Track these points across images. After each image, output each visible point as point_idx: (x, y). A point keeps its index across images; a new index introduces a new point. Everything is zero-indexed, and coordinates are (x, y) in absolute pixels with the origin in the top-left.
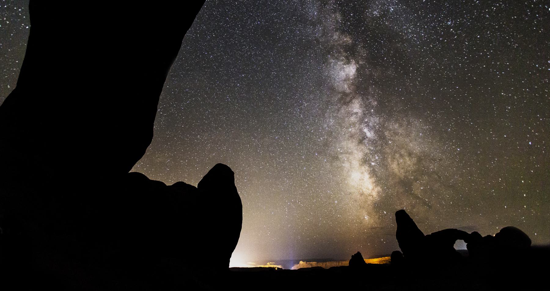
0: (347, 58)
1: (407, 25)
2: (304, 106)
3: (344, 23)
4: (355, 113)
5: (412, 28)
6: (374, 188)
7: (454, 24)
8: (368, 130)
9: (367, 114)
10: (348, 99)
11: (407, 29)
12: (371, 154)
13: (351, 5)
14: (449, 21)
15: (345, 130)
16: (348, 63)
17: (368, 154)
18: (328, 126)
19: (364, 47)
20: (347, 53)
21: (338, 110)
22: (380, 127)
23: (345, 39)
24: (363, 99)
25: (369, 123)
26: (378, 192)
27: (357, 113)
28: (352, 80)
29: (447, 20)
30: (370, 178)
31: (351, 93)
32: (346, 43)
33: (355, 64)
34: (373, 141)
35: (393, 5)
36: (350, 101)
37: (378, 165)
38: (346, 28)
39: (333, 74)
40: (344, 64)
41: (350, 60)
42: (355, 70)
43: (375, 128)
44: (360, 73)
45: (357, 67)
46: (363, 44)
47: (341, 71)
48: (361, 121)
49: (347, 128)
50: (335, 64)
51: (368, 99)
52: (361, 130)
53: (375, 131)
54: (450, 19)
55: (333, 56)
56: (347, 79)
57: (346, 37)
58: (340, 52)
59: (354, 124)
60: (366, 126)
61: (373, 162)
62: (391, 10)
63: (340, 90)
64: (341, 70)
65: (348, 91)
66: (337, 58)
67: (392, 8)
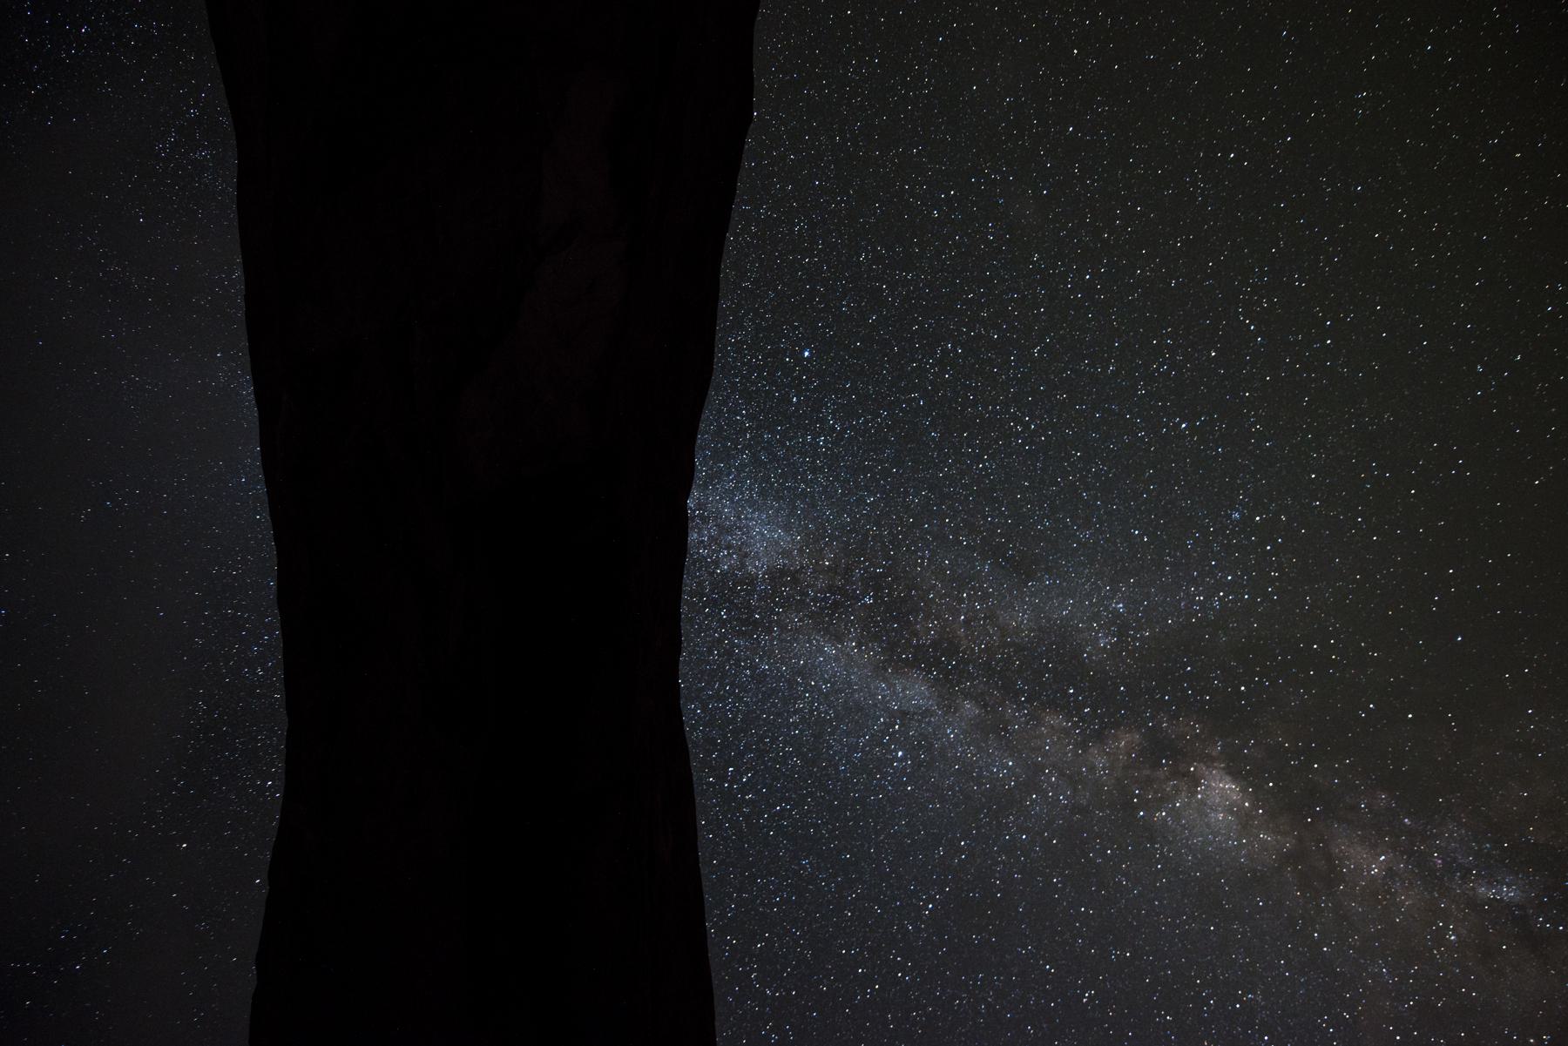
0: (1176, 773)
11: (1193, 602)
13: (1048, 678)
28: (1255, 807)
29: (1224, 517)
32: (1133, 748)
38: (1095, 724)
39: (1203, 842)
42: (1228, 778)
45: (1224, 769)
47: (1206, 816)
52: (1474, 904)
54: (1226, 511)
56: (1245, 822)
57: (1116, 738)
60: (1462, 878)
62: (1121, 608)
67: (1117, 603)
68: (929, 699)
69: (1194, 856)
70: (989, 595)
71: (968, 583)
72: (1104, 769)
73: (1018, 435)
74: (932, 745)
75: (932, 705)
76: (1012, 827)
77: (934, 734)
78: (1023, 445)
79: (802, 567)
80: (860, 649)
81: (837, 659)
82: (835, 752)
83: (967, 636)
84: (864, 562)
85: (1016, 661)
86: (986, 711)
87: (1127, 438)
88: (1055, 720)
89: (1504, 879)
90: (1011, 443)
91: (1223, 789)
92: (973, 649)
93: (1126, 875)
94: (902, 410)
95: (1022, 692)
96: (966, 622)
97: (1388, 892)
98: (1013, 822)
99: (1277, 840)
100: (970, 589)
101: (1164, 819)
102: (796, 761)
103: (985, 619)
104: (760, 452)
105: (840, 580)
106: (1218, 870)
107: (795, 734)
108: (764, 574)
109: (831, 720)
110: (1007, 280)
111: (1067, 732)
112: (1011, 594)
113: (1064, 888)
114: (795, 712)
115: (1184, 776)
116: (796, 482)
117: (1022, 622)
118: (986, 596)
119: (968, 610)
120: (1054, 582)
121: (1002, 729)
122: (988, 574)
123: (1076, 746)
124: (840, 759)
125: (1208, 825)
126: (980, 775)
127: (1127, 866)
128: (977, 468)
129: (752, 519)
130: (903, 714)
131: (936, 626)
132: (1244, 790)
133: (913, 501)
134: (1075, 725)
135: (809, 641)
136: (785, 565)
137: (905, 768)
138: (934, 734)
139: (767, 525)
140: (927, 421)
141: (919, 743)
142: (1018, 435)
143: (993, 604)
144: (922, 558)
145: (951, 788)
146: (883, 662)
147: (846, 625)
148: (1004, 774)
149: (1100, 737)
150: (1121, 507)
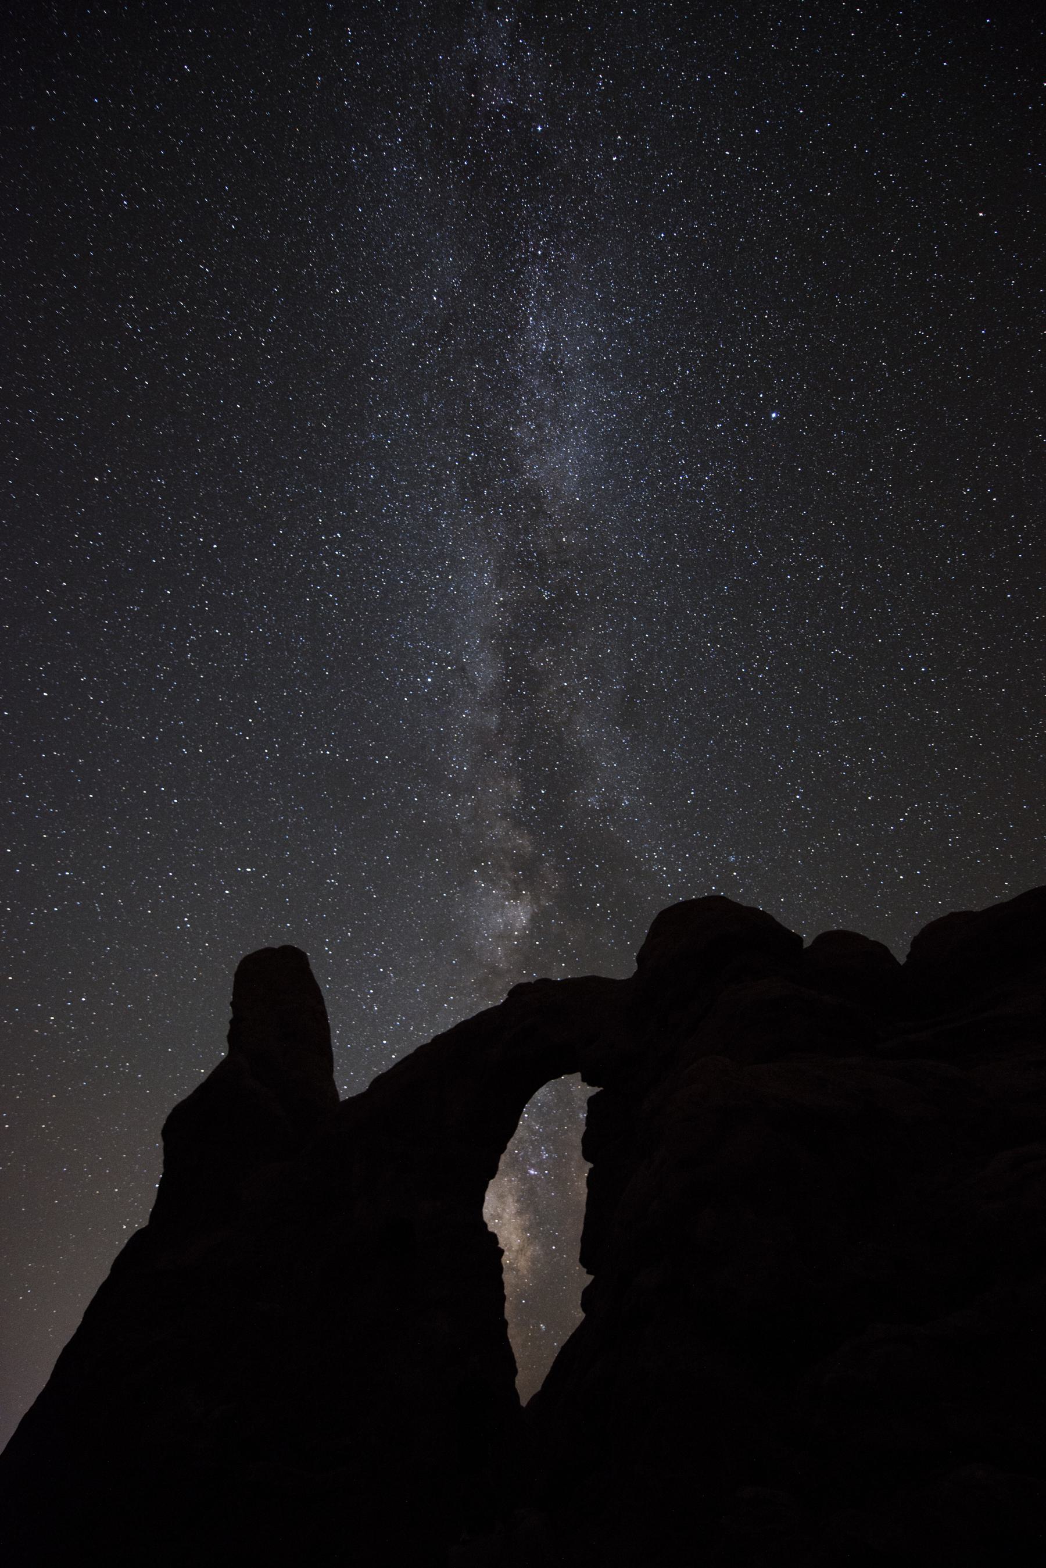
0: (515, 883)
1: (651, 841)
2: (389, 984)
3: (522, 806)
5: (661, 851)
6: (524, 1246)
7: (740, 862)
11: (650, 851)
12: (532, 1142)
13: (545, 771)
14: (732, 855)
16: (517, 896)
17: (526, 1141)
19: (557, 869)
20: (517, 872)
26: (534, 1260)
28: (517, 938)
30: (519, 1213)
31: (509, 971)
33: (530, 902)
34: (542, 1106)
35: (630, 794)
37: (545, 1175)
42: (529, 916)
44: (539, 928)
45: (534, 910)
54: (733, 850)
55: (484, 874)
56: (504, 936)
57: (521, 837)
61: (533, 1166)
62: (625, 803)
67: (628, 800)
69: (463, 914)
70: (594, 699)
73: (749, 666)
74: (449, 703)
75: (481, 689)
77: (459, 701)
78: (741, 674)
79: (550, 517)
80: (499, 607)
81: (482, 589)
82: (401, 625)
83: (550, 694)
86: (498, 734)
87: (773, 758)
88: (515, 788)
90: (740, 663)
91: (520, 916)
93: (427, 876)
94: (741, 546)
99: (501, 958)
100: (593, 681)
102: (377, 593)
103: (572, 703)
104: (651, 413)
106: (462, 930)
107: (399, 581)
108: (528, 480)
109: (426, 608)
111: (509, 799)
113: (395, 840)
114: (418, 573)
115: (516, 888)
116: (632, 469)
117: (582, 733)
120: (627, 746)
121: (488, 752)
122: (612, 690)
124: (399, 632)
125: (490, 915)
129: (577, 439)
130: (463, 669)
131: (548, 665)
132: (525, 928)
133: (654, 597)
134: (518, 804)
135: (485, 557)
136: (545, 497)
137: (419, 688)
138: (459, 701)
139: (577, 458)
140: (737, 577)
141: (446, 692)
142: (749, 666)
143: (587, 705)
145: (423, 731)
147: (515, 584)
149: (517, 824)
150: (710, 774)
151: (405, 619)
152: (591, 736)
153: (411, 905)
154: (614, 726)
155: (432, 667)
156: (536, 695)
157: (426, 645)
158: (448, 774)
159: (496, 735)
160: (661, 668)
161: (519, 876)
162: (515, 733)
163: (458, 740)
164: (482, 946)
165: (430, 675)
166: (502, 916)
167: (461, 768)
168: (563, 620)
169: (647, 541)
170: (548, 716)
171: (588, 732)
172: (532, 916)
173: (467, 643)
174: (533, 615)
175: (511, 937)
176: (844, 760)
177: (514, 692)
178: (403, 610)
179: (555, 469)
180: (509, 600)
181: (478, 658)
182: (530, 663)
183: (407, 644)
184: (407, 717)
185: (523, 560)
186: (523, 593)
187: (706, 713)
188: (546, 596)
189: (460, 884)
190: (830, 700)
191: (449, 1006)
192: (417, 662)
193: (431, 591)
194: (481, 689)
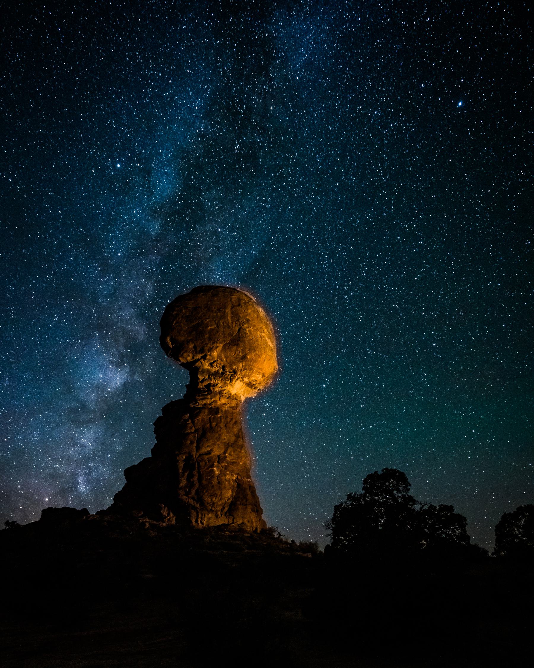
0: (122, 356)
4: (80, 444)
8: (85, 482)
9: (99, 457)
10: (83, 417)
15: (49, 461)
16: (119, 365)
18: (23, 440)
20: (126, 349)
21: (58, 425)
22: (104, 486)
23: (138, 327)
24: (106, 429)
25: (94, 471)
27: (85, 447)
28: (108, 393)
31: (94, 411)
32: (135, 335)
33: (128, 374)
34: (82, 501)
36: (88, 422)
40: (112, 363)
41: (125, 363)
42: (122, 382)
43: (97, 483)
46: (157, 354)
47: (100, 369)
48: (85, 460)
49: (55, 461)
50: (99, 353)
51: (113, 435)
52: (75, 475)
53: (94, 488)
58: (116, 341)
59: (69, 460)
60: (87, 473)
63: (82, 397)
64: (101, 367)
65: (91, 406)
66: (106, 347)
68: (160, 195)
69: (76, 360)
70: (234, 252)
71: (243, 237)
72: (121, 315)
73: (342, 286)
74: (127, 194)
75: (156, 197)
76: (76, 251)
77: (135, 198)
78: (335, 289)
79: (271, 79)
80: (199, 135)
81: (191, 110)
82: (113, 101)
83: (206, 232)
84: (269, 147)
85: (188, 266)
86: (154, 241)
87: (324, 355)
88: (150, 289)
89: (88, 486)
90: (338, 280)
91: (116, 379)
92: (197, 236)
93: (59, 322)
94: (384, 196)
95: (168, 268)
96: (216, 233)
97: (74, 445)
98: (80, 251)
99: (92, 401)
100: (239, 238)
101: (96, 347)
102: (103, 56)
103: (218, 247)
104: (385, 38)
105: (256, 121)
108: (269, 31)
109: (140, 99)
110: (453, 292)
111: (143, 294)
112: (234, 268)
113: (44, 282)
114: (145, 59)
115: (122, 360)
116: (348, 79)
118: (234, 251)
119: (223, 234)
121: (141, 251)
122: (248, 252)
123: (134, 300)
124: (109, 106)
125: (95, 369)
126: (108, 231)
127: (65, 323)
128: (325, 253)
129: (323, 21)
130: (148, 172)
132: (116, 389)
133: (310, 198)
134: (147, 301)
135: (206, 82)
136: (275, 58)
137: (108, 168)
138: (135, 198)
139: (315, 39)
140: (369, 218)
141: (128, 183)
142: (342, 286)
144: (266, 201)
145: (98, 206)
146: (187, 157)
147: (218, 123)
148: (111, 249)
149: (141, 315)
151: (118, 97)
152: (219, 278)
153: (40, 336)
154: (238, 280)
155: (124, 155)
156: (195, 226)
157: (128, 132)
158: (104, 252)
159: (153, 241)
160: (289, 255)
161: (127, 352)
162: (167, 247)
163: (122, 229)
164: (81, 387)
165: (120, 162)
166: (104, 374)
167: (116, 253)
168: (240, 178)
169: (328, 151)
170: (196, 246)
171: (218, 275)
172: (125, 383)
173: (160, 151)
174: (221, 159)
175: (104, 390)
176: (361, 376)
177: (180, 215)
178: (120, 88)
179: (293, 37)
180: (208, 134)
181: (164, 170)
182: (202, 197)
183: (111, 121)
184: (88, 186)
185: (234, 106)
186: (220, 135)
187: (300, 304)
188: (237, 149)
189: (82, 338)
190: (375, 335)
191: (43, 417)
192: (114, 143)
193: (148, 84)
194: (156, 197)
